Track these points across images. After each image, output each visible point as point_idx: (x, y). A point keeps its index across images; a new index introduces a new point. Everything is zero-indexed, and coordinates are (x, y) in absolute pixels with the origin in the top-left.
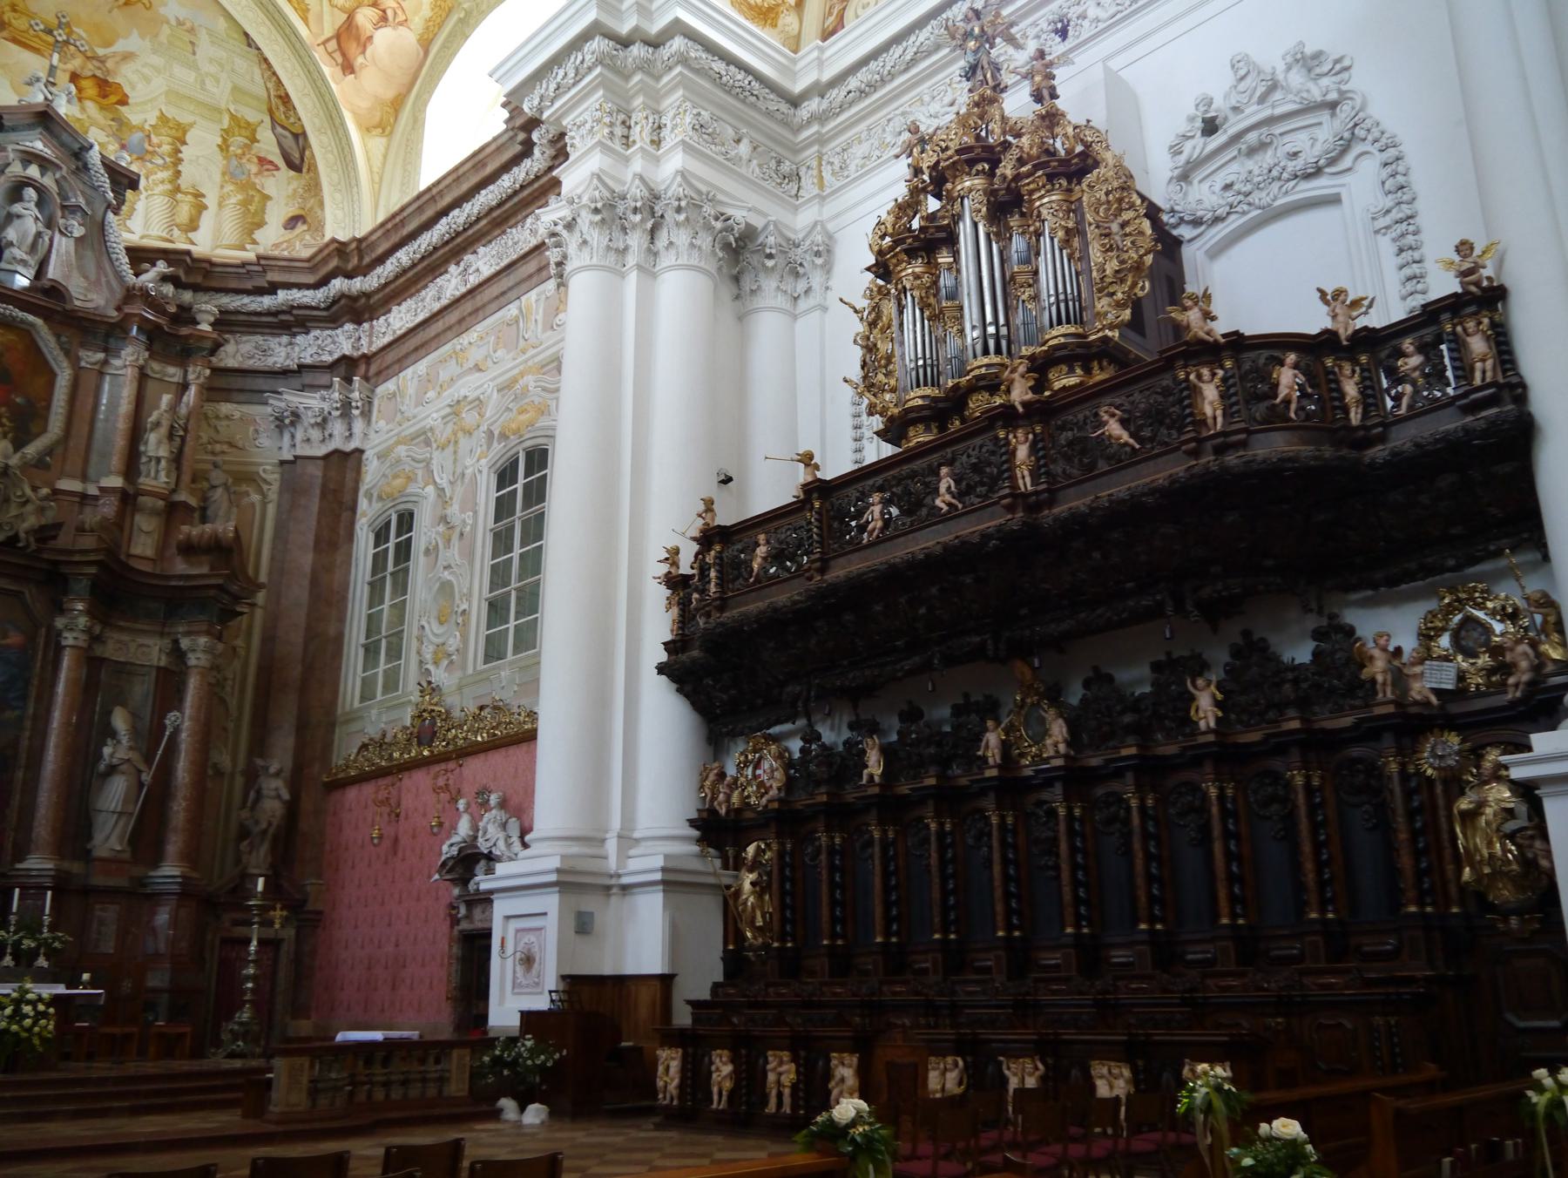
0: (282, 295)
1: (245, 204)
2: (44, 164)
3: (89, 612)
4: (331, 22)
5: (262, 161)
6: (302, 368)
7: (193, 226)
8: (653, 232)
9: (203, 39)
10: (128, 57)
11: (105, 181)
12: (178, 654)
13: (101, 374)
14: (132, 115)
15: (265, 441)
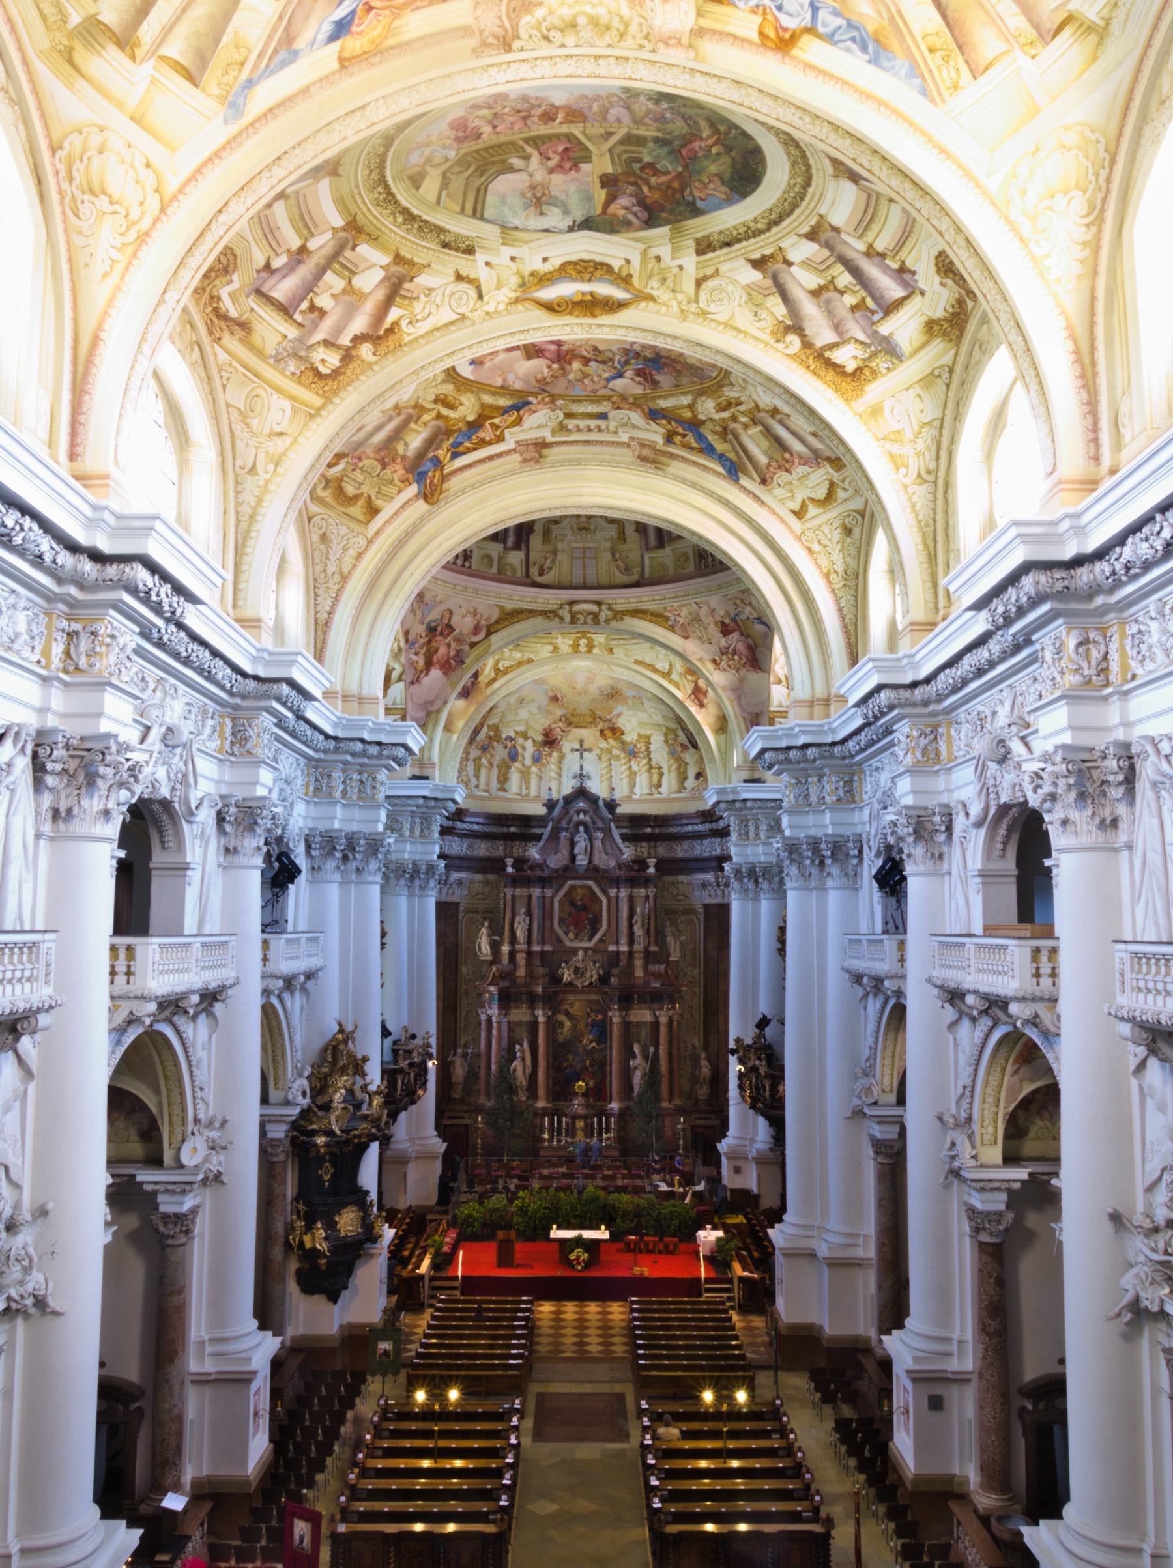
0: (690, 828)
1: (679, 768)
2: (585, 812)
3: (620, 1009)
4: (689, 688)
5: (683, 745)
6: (704, 860)
7: (659, 785)
8: (757, 882)
9: (645, 701)
10: (619, 715)
11: (605, 813)
12: (657, 1018)
13: (617, 897)
14: (628, 738)
15: (697, 893)
